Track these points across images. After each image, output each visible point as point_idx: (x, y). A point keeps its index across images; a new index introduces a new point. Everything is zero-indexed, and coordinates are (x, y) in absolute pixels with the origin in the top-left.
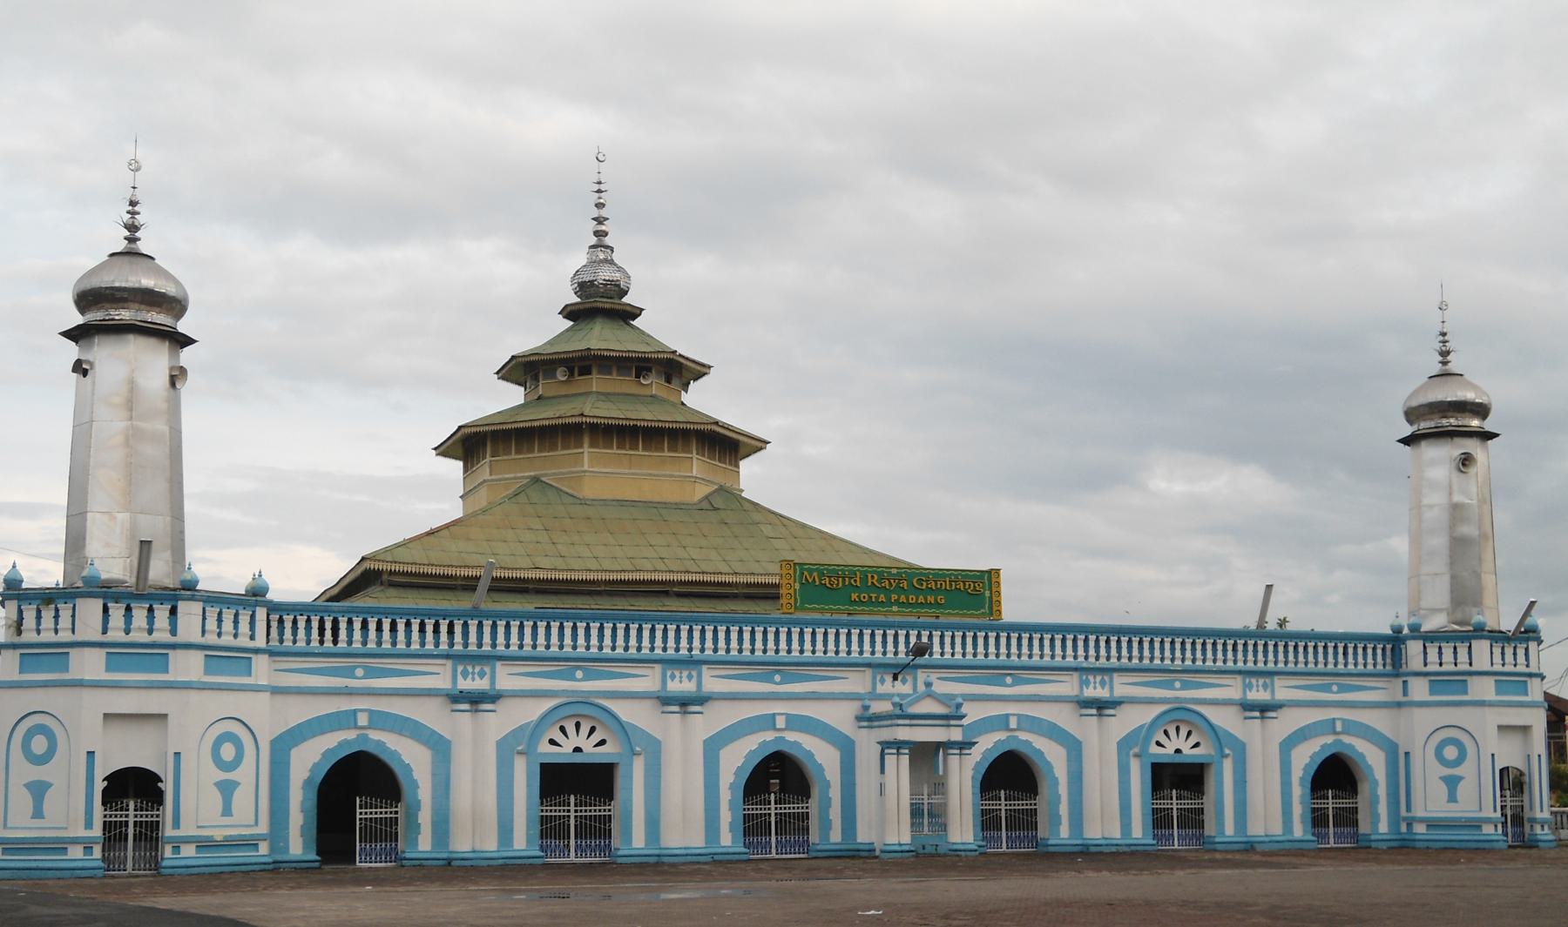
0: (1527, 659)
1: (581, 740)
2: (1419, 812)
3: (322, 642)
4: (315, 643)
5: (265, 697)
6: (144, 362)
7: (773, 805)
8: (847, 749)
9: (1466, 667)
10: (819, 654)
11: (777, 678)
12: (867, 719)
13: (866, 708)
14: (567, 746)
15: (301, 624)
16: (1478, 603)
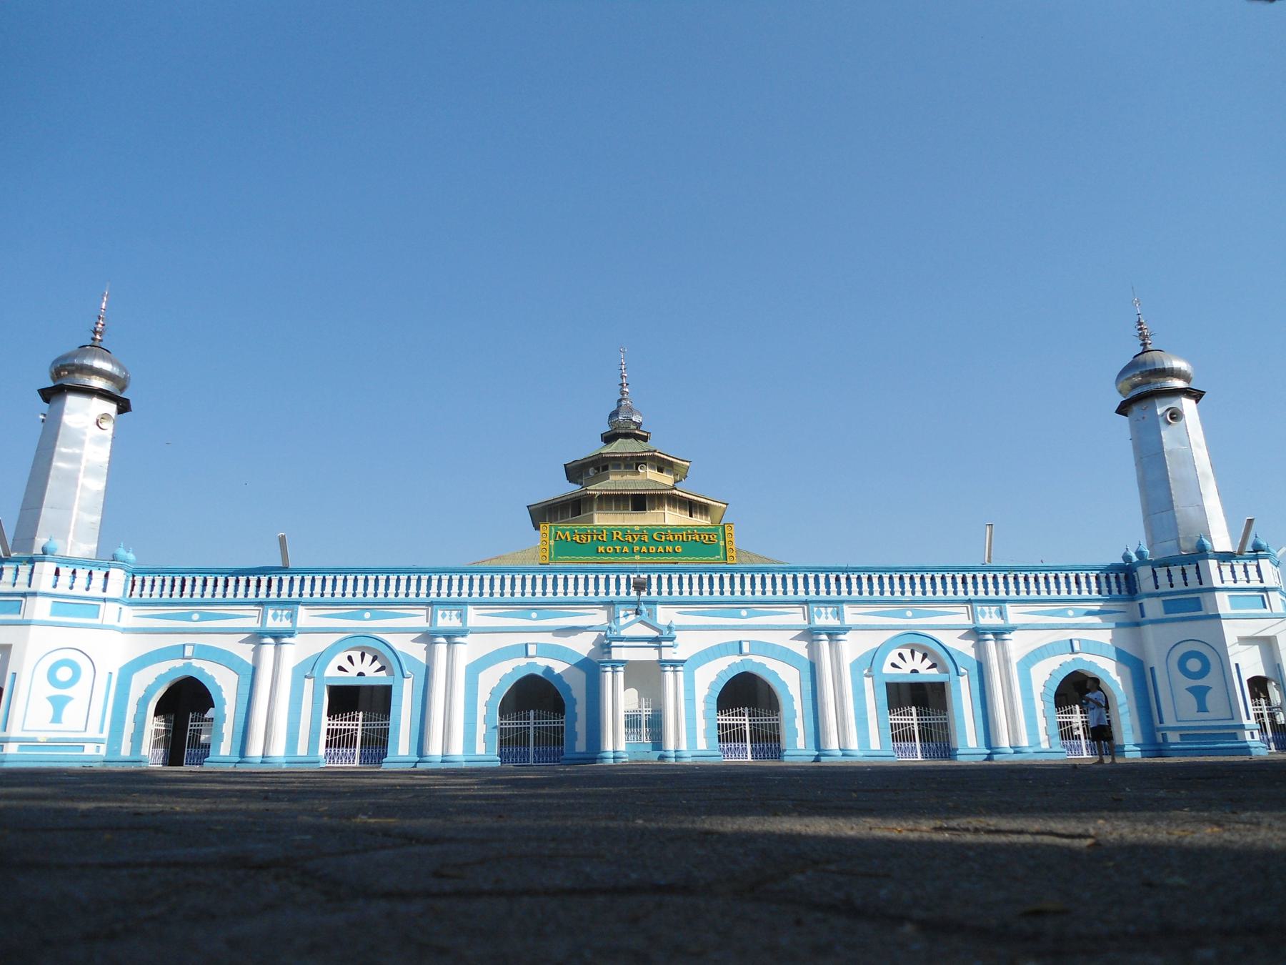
0: (1260, 575)
7: (532, 721)
11: (534, 615)
14: (353, 671)
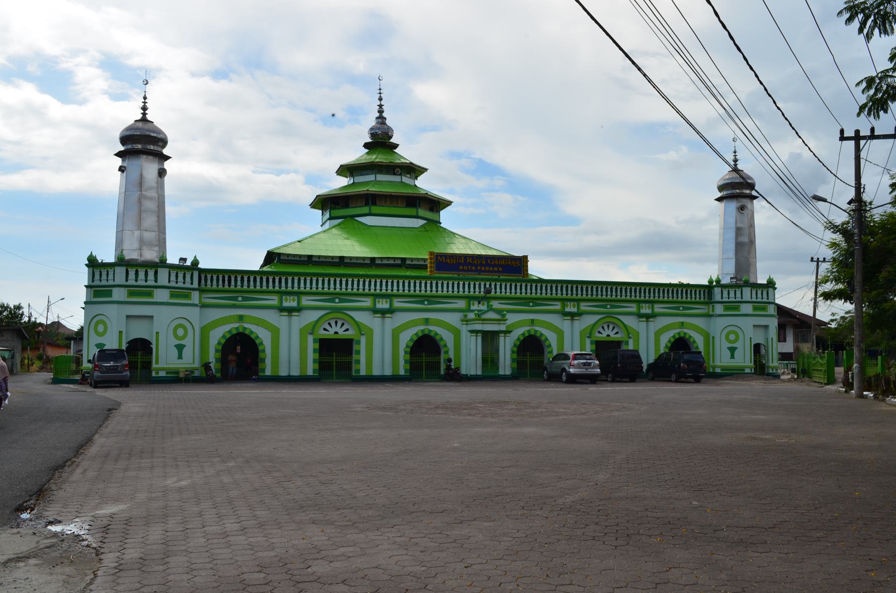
1: (338, 329)
2: (718, 363)
3: (223, 286)
4: (221, 286)
5: (197, 309)
6: (150, 168)
8: (457, 333)
9: (740, 299)
10: (450, 292)
12: (466, 321)
13: (466, 316)
14: (332, 331)
15: (215, 278)
16: (748, 272)
